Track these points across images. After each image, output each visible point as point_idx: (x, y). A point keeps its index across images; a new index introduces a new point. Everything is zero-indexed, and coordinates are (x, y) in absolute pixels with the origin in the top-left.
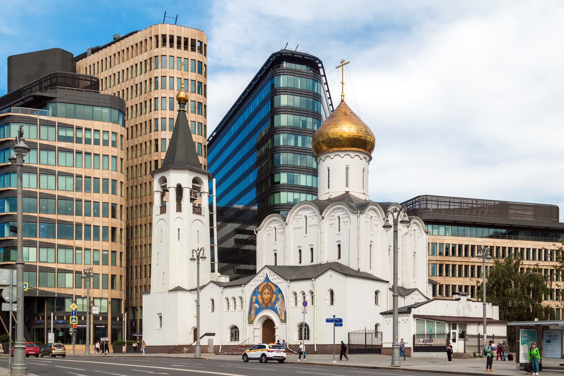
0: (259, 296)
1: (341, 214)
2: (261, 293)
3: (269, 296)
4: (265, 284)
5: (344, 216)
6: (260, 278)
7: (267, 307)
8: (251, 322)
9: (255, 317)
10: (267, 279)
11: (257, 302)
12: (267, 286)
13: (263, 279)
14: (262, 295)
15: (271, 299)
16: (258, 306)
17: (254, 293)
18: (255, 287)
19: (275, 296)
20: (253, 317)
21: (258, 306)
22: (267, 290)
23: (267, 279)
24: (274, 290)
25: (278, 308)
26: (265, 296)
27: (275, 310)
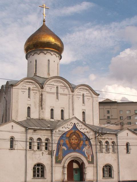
0: (67, 141)
1: (31, 87)
2: (69, 138)
3: (76, 141)
4: (73, 131)
5: (87, 94)
6: (69, 126)
7: (74, 150)
8: (58, 161)
9: (63, 157)
10: (75, 126)
11: (64, 144)
12: (74, 133)
13: (71, 127)
14: (70, 140)
15: (78, 144)
16: (66, 149)
17: (61, 138)
18: (64, 132)
19: (82, 143)
20: (60, 158)
21: (66, 149)
22: (74, 136)
23: (75, 126)
24: (82, 137)
25: (85, 152)
26: (73, 142)
27: (83, 154)
